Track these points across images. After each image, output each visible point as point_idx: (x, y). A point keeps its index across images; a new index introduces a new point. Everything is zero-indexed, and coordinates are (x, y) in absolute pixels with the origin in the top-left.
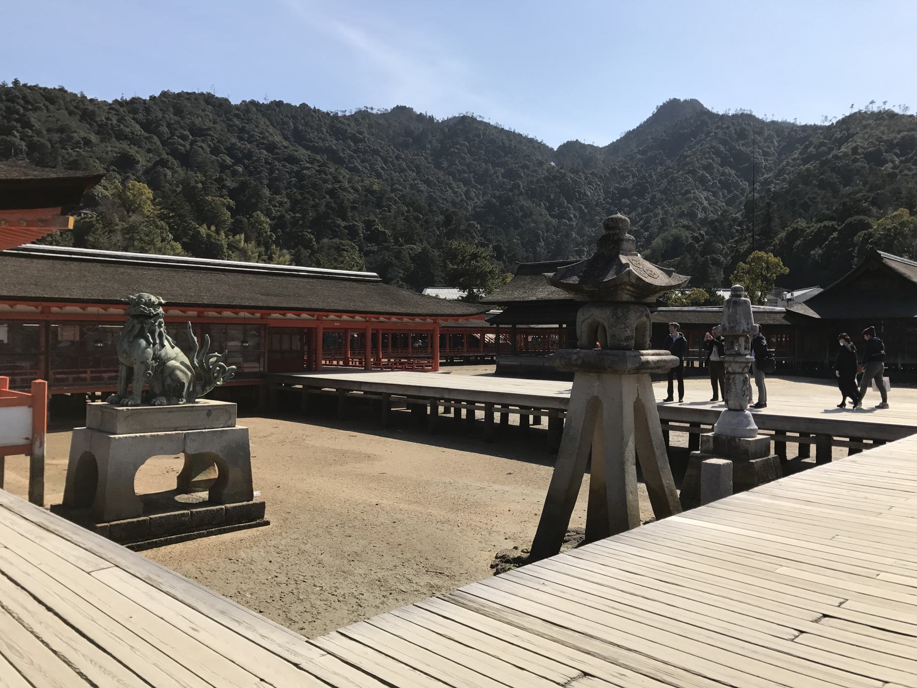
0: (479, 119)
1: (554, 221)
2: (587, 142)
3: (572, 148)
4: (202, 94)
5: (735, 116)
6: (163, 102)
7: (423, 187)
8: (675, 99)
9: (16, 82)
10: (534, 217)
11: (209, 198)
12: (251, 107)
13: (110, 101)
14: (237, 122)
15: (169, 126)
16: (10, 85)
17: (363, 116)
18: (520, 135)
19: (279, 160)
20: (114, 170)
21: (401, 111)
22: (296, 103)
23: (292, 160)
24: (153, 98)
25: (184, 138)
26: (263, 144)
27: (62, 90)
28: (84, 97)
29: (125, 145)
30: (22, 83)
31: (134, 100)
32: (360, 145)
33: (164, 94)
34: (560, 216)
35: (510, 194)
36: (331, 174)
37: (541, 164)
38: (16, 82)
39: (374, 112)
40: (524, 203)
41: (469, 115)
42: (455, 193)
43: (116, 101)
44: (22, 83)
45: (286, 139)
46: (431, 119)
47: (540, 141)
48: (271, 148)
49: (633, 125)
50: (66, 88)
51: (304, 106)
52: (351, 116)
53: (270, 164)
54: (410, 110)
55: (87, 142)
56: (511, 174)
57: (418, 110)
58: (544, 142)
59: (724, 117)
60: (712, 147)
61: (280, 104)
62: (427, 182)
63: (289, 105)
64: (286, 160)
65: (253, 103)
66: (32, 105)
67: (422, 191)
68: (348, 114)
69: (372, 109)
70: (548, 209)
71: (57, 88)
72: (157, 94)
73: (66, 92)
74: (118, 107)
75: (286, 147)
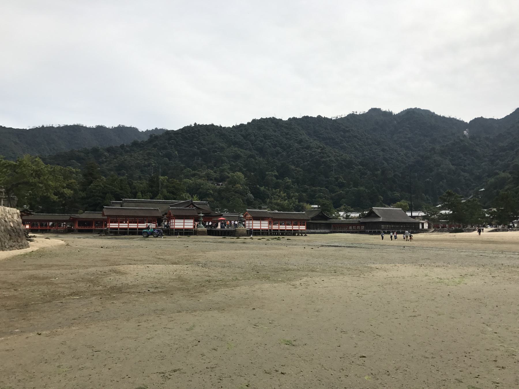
1: (453, 167)
2: (488, 117)
6: (253, 125)
7: (381, 153)
9: (195, 124)
10: (442, 166)
11: (267, 173)
12: (293, 120)
14: (285, 130)
15: (255, 136)
17: (352, 117)
19: (303, 148)
20: (232, 161)
22: (315, 115)
23: (308, 147)
24: (248, 123)
25: (261, 141)
26: (297, 140)
27: (213, 125)
28: (221, 127)
29: (236, 149)
31: (242, 125)
32: (347, 134)
33: (254, 121)
35: (429, 154)
36: (326, 153)
38: (195, 124)
39: (358, 114)
42: (399, 154)
45: (309, 134)
46: (390, 114)
48: (300, 142)
51: (319, 117)
53: (298, 150)
54: (379, 109)
55: (222, 149)
61: (307, 117)
62: (383, 150)
63: (311, 117)
64: (306, 148)
65: (294, 118)
67: (380, 156)
68: (343, 117)
72: (250, 121)
75: (307, 141)
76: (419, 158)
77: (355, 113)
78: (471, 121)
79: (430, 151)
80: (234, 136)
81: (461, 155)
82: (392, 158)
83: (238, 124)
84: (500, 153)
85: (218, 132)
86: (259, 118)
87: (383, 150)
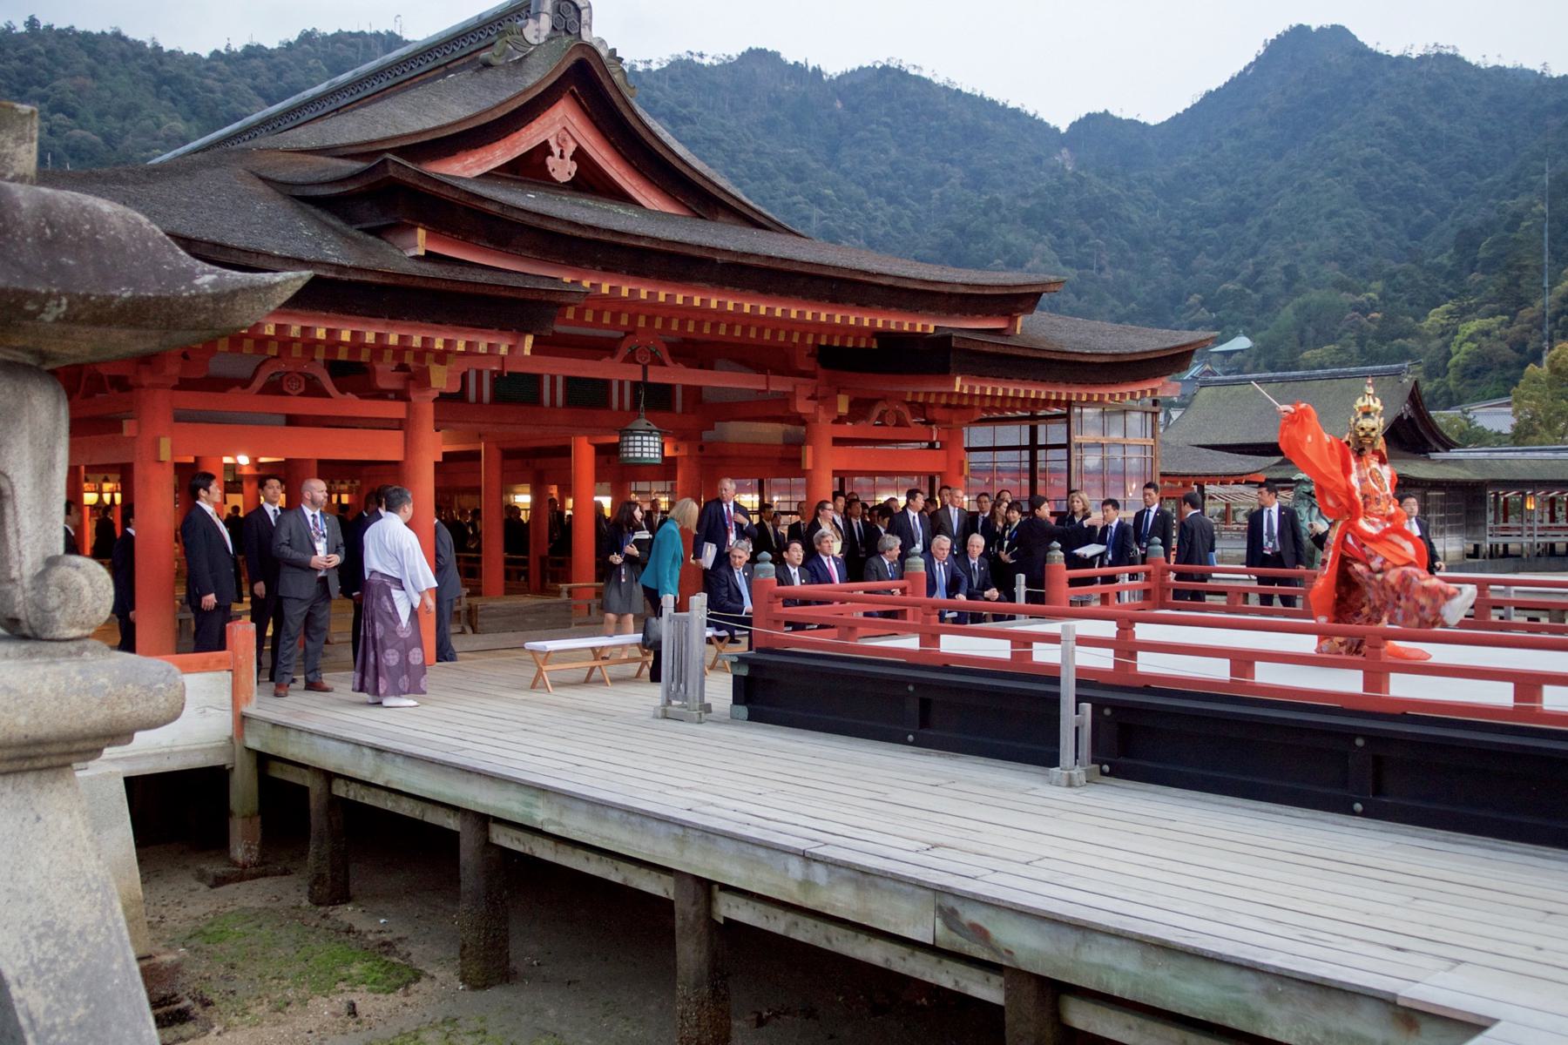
0: (912, 72)
3: (1096, 127)
4: (378, 34)
5: (1423, 59)
8: (1301, 26)
9: (32, 23)
13: (205, 54)
16: (21, 28)
18: (993, 103)
21: (757, 56)
28: (157, 49)
30: (43, 24)
33: (307, 37)
34: (1082, 264)
37: (1038, 160)
38: (32, 23)
39: (706, 61)
40: (1011, 237)
41: (894, 65)
42: (874, 219)
43: (216, 54)
44: (43, 24)
46: (817, 72)
47: (1031, 113)
49: (1216, 81)
50: (125, 32)
52: (662, 70)
54: (775, 56)
56: (977, 180)
57: (790, 57)
58: (1040, 116)
59: (1401, 61)
60: (1382, 124)
66: (66, 68)
68: (655, 67)
69: (701, 56)
70: (1054, 247)
71: (108, 31)
73: (125, 39)
74: (221, 65)
76: (951, 234)
77: (697, 59)
78: (1073, 125)
79: (985, 214)
80: (225, 93)
81: (1085, 228)
82: (851, 232)
83: (238, 46)
84: (1207, 231)
85: (150, 68)
86: (328, 28)
87: (818, 200)
